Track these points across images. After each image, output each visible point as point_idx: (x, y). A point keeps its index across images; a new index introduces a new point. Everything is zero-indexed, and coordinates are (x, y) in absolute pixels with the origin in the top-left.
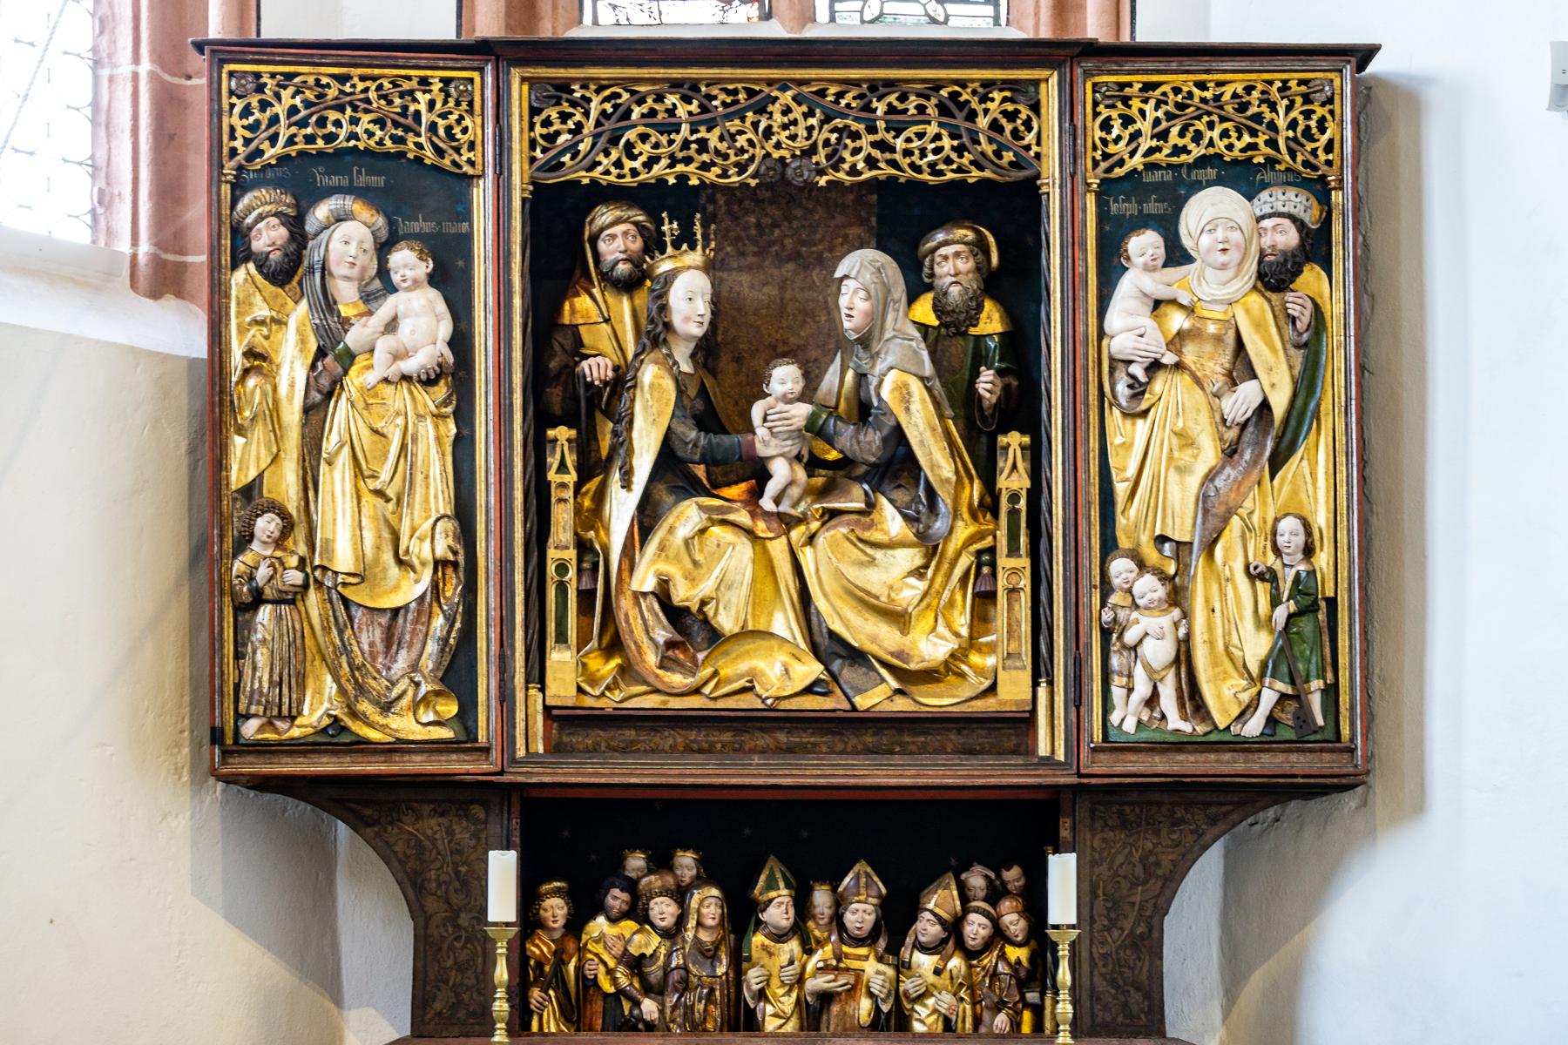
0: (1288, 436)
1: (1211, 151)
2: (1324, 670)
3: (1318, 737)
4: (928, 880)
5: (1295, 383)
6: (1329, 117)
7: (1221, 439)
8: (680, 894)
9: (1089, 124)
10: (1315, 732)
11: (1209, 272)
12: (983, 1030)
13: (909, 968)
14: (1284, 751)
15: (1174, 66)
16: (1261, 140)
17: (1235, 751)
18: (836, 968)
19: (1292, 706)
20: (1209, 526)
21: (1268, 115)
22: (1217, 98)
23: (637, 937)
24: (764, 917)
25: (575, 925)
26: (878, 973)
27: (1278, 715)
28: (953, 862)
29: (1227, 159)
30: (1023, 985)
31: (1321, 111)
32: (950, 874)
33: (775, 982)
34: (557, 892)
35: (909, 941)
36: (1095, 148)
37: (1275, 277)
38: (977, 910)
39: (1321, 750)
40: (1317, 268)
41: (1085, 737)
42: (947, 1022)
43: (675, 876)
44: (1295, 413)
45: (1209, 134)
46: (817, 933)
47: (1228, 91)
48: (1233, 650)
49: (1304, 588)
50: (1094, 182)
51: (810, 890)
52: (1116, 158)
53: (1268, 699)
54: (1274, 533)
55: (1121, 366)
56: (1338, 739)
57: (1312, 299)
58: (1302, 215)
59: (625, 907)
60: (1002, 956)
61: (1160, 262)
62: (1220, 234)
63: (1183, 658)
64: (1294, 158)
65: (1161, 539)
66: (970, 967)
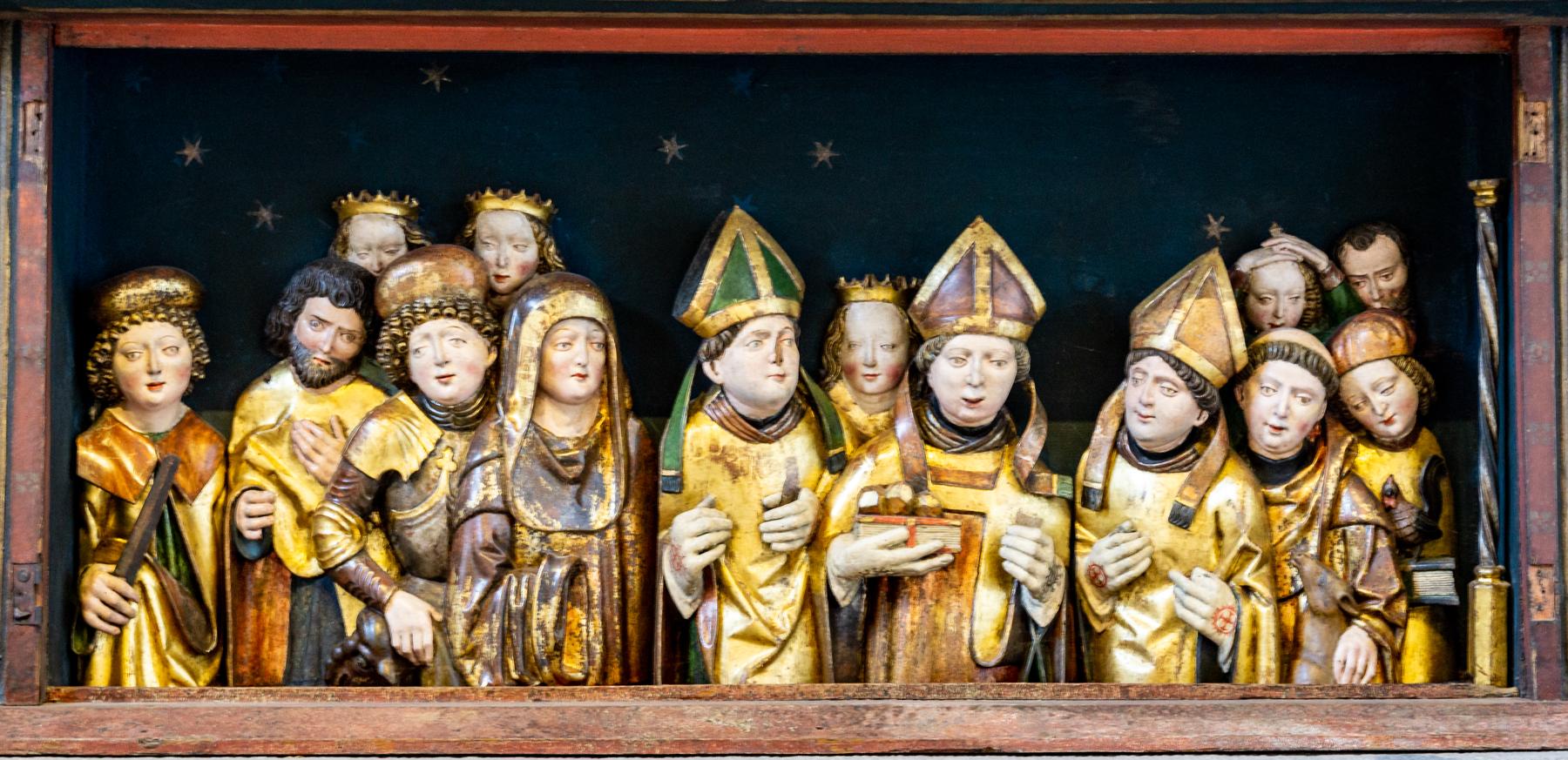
4: (1155, 269)
8: (493, 311)
12: (1304, 673)
13: (1104, 507)
18: (912, 510)
23: (375, 428)
24: (717, 372)
25: (213, 397)
26: (1022, 520)
28: (1215, 228)
30: (1405, 550)
32: (1214, 256)
33: (747, 547)
34: (162, 306)
35: (1103, 434)
38: (1288, 353)
42: (1207, 646)
43: (483, 266)
46: (858, 415)
51: (839, 301)
59: (347, 349)
60: (1349, 476)
66: (1267, 502)
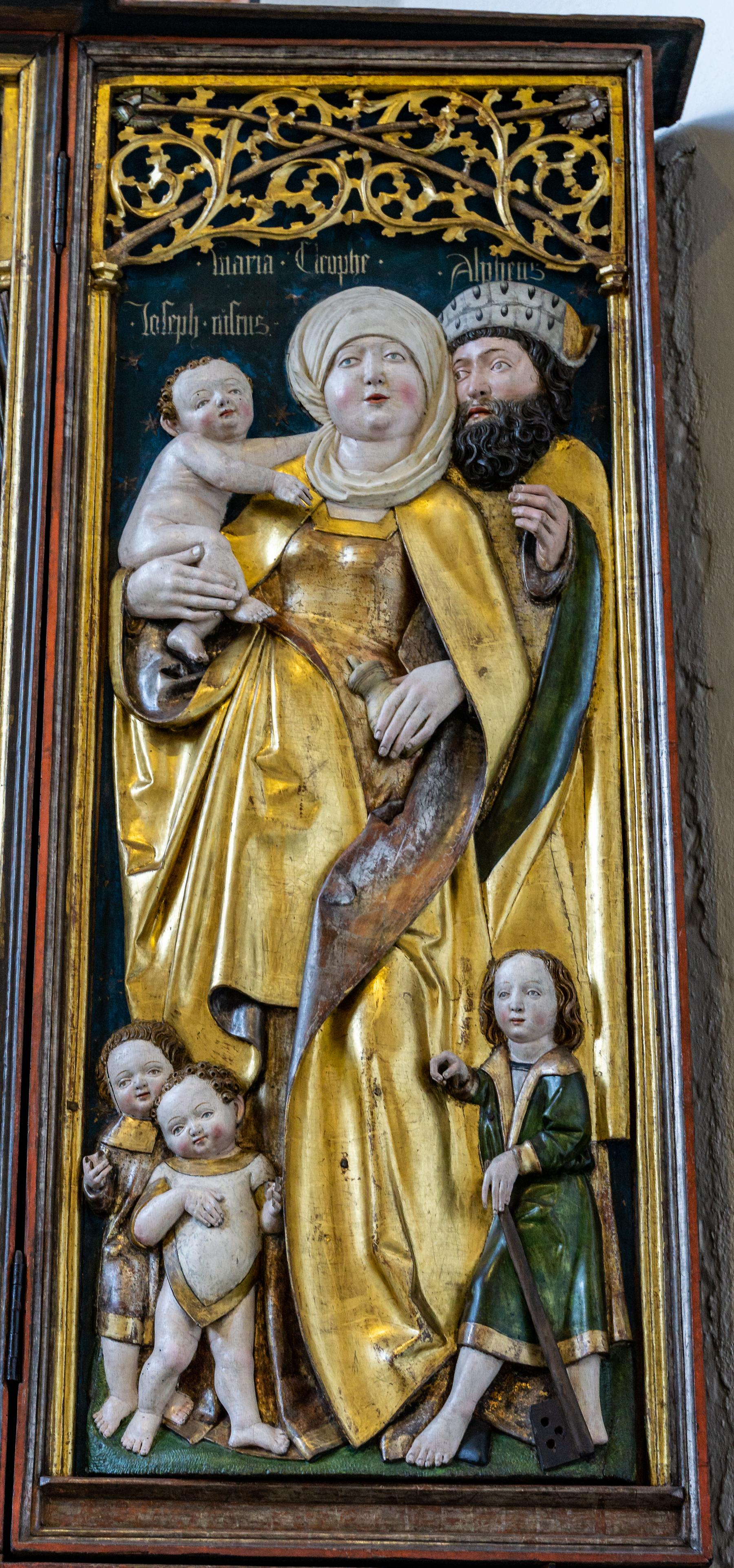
0: (519, 787)
1: (354, 216)
2: (606, 1308)
3: (594, 1469)
5: (533, 673)
6: (598, 156)
7: (367, 785)
9: (101, 159)
10: (586, 1458)
11: (349, 449)
14: (511, 1504)
15: (279, 56)
16: (458, 199)
17: (391, 1501)
19: (531, 1394)
20: (336, 969)
21: (472, 153)
22: (368, 119)
27: (495, 1414)
29: (389, 232)
31: (580, 146)
36: (111, 206)
37: (489, 458)
39: (602, 1504)
40: (582, 446)
41: (28, 1460)
44: (532, 733)
45: (349, 184)
47: (392, 108)
48: (389, 1255)
49: (559, 1116)
50: (107, 268)
52: (153, 227)
53: (473, 1373)
54: (488, 993)
55: (152, 634)
56: (644, 1477)
57: (570, 506)
58: (543, 333)
61: (243, 421)
62: (368, 367)
63: (269, 1273)
64: (530, 238)
65: (227, 999)
